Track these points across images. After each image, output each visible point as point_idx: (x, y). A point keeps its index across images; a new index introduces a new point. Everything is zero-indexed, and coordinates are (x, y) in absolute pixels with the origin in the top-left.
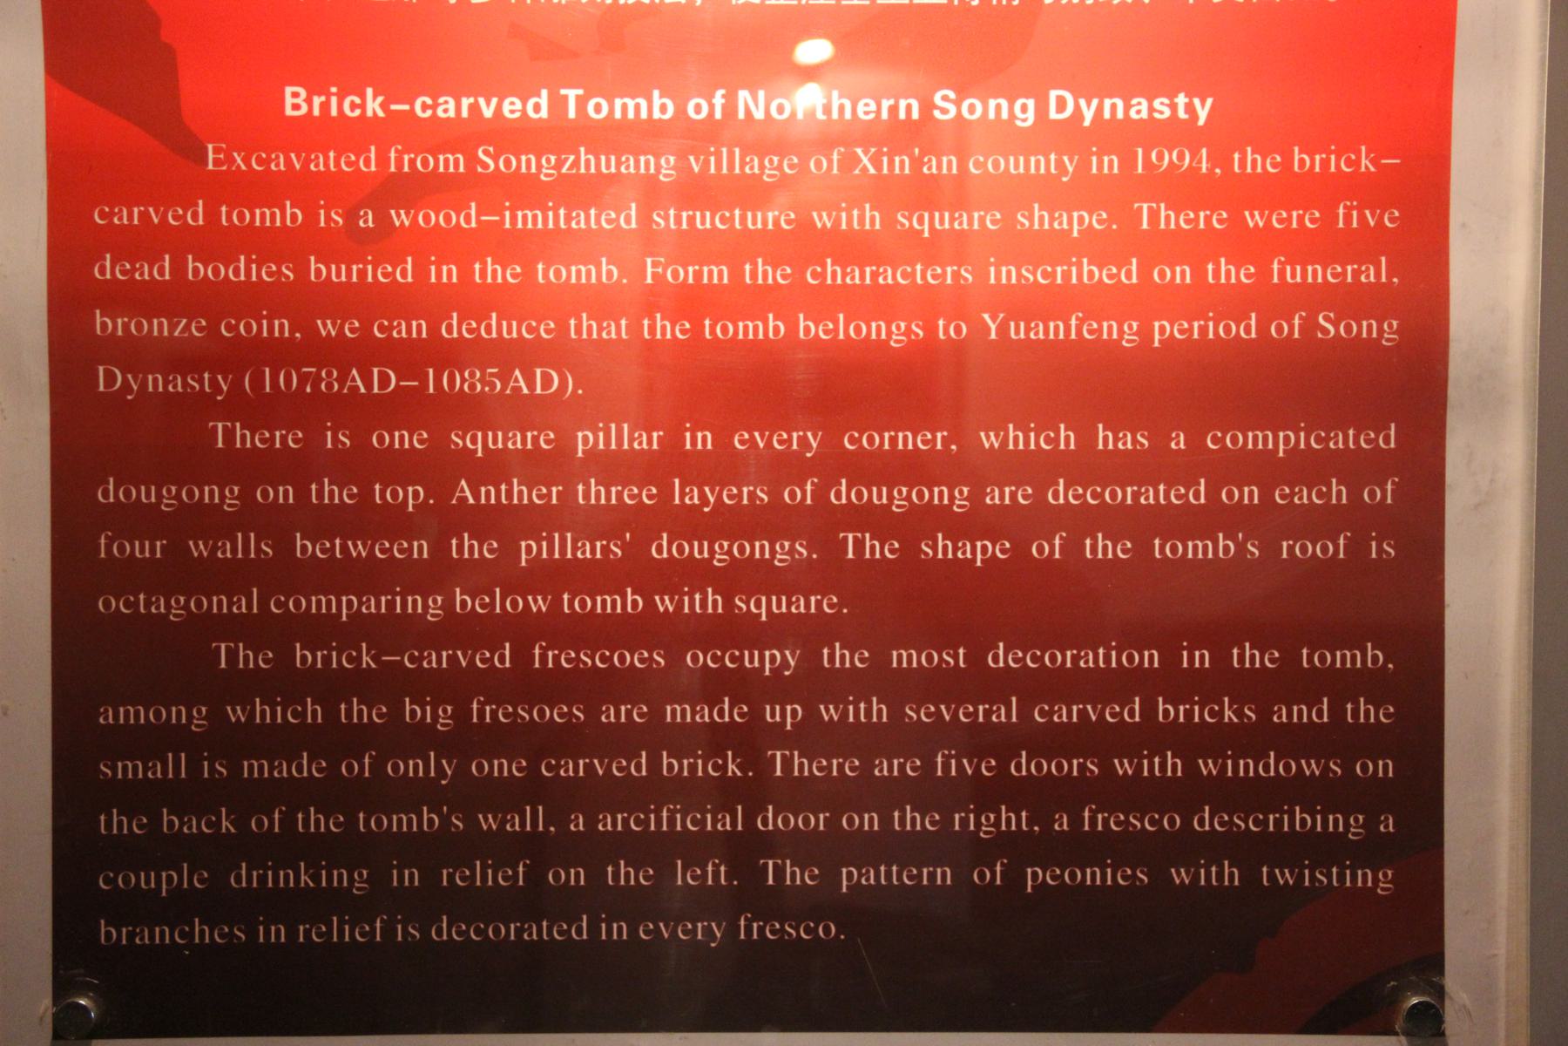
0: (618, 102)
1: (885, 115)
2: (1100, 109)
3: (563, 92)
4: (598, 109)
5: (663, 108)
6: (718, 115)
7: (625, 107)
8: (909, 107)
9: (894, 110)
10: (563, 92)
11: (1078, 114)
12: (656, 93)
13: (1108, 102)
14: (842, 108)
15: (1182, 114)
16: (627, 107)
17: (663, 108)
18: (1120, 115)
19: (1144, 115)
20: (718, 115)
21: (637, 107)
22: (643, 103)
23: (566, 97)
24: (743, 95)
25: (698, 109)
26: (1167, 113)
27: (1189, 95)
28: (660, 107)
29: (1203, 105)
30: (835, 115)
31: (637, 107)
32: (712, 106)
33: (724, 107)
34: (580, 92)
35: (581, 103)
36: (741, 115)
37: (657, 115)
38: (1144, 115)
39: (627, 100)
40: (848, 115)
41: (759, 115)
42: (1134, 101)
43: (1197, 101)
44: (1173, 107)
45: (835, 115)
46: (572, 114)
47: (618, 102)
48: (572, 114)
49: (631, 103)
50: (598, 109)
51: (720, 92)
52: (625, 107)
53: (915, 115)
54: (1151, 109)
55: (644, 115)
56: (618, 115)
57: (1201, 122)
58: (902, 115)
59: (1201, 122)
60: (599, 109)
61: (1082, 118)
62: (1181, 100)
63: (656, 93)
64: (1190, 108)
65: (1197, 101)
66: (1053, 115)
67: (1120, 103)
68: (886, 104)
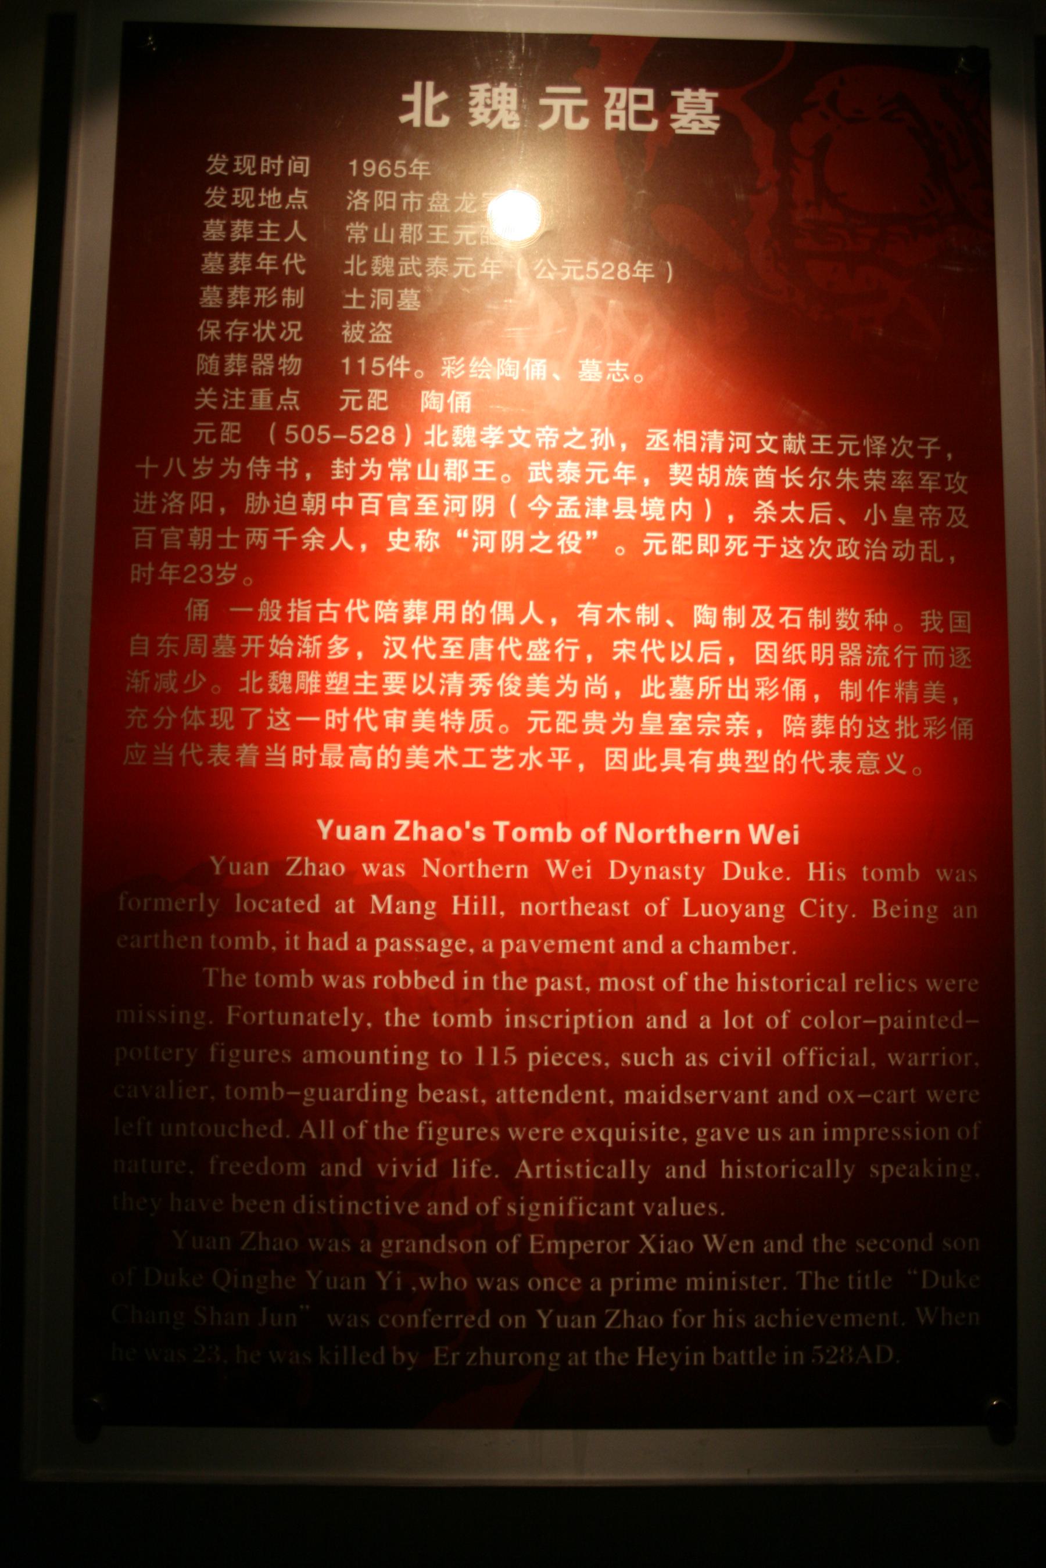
0: (533, 831)
1: (716, 841)
3: (496, 823)
4: (520, 834)
5: (564, 835)
6: (602, 839)
7: (537, 834)
8: (733, 836)
9: (722, 837)
10: (496, 823)
12: (559, 824)
14: (687, 835)
16: (540, 833)
17: (564, 835)
20: (602, 839)
21: (546, 834)
22: (550, 831)
23: (497, 827)
24: (620, 826)
25: (588, 835)
28: (562, 833)
30: (682, 840)
31: (546, 834)
32: (598, 834)
33: (606, 834)
34: (507, 823)
35: (508, 831)
36: (618, 840)
37: (560, 839)
39: (539, 829)
40: (691, 841)
41: (630, 839)
45: (682, 840)
46: (501, 838)
47: (533, 831)
48: (501, 838)
50: (520, 834)
51: (603, 824)
52: (537, 834)
53: (737, 841)
55: (551, 839)
56: (533, 839)
58: (728, 841)
60: (520, 835)
63: (559, 824)
68: (717, 833)
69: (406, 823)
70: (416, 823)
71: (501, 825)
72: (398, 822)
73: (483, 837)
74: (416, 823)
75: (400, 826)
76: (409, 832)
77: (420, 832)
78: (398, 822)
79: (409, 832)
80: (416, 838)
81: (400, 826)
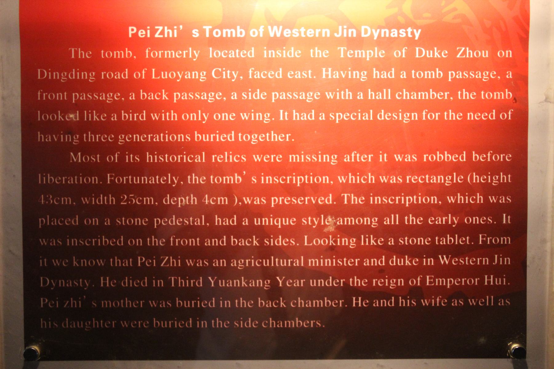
0: (224, 31)
2: (380, 33)
4: (217, 33)
5: (241, 33)
6: (261, 35)
7: (227, 32)
10: (204, 27)
11: (372, 34)
12: (238, 27)
13: (383, 31)
15: (410, 36)
17: (241, 33)
18: (387, 35)
19: (396, 36)
20: (261, 35)
21: (231, 33)
22: (233, 31)
23: (205, 30)
25: (254, 33)
26: (405, 35)
27: (413, 28)
29: (417, 31)
31: (231, 33)
35: (211, 31)
37: (239, 35)
38: (396, 36)
42: (392, 30)
43: (415, 31)
44: (407, 32)
46: (207, 35)
48: (207, 35)
49: (229, 31)
50: (217, 33)
52: (227, 32)
54: (399, 34)
55: (234, 36)
57: (417, 38)
59: (417, 38)
61: (374, 37)
62: (409, 30)
64: (412, 33)
65: (415, 31)
66: (363, 35)
67: (387, 31)
69: (161, 28)
70: (166, 28)
71: (207, 28)
72: (156, 27)
73: (198, 35)
74: (166, 28)
75: (158, 29)
76: (162, 33)
77: (168, 33)
78: (156, 27)
79: (162, 33)
80: (166, 36)
81: (158, 29)
